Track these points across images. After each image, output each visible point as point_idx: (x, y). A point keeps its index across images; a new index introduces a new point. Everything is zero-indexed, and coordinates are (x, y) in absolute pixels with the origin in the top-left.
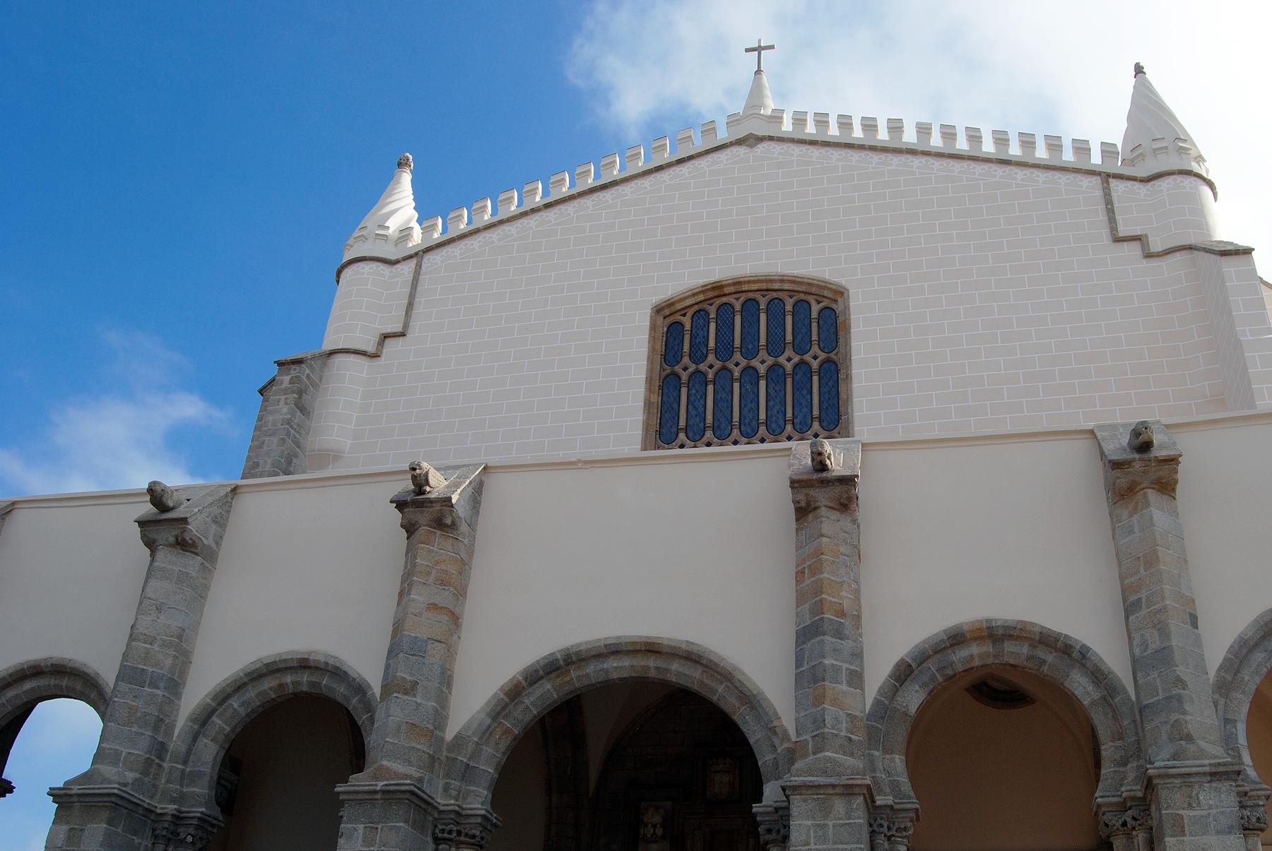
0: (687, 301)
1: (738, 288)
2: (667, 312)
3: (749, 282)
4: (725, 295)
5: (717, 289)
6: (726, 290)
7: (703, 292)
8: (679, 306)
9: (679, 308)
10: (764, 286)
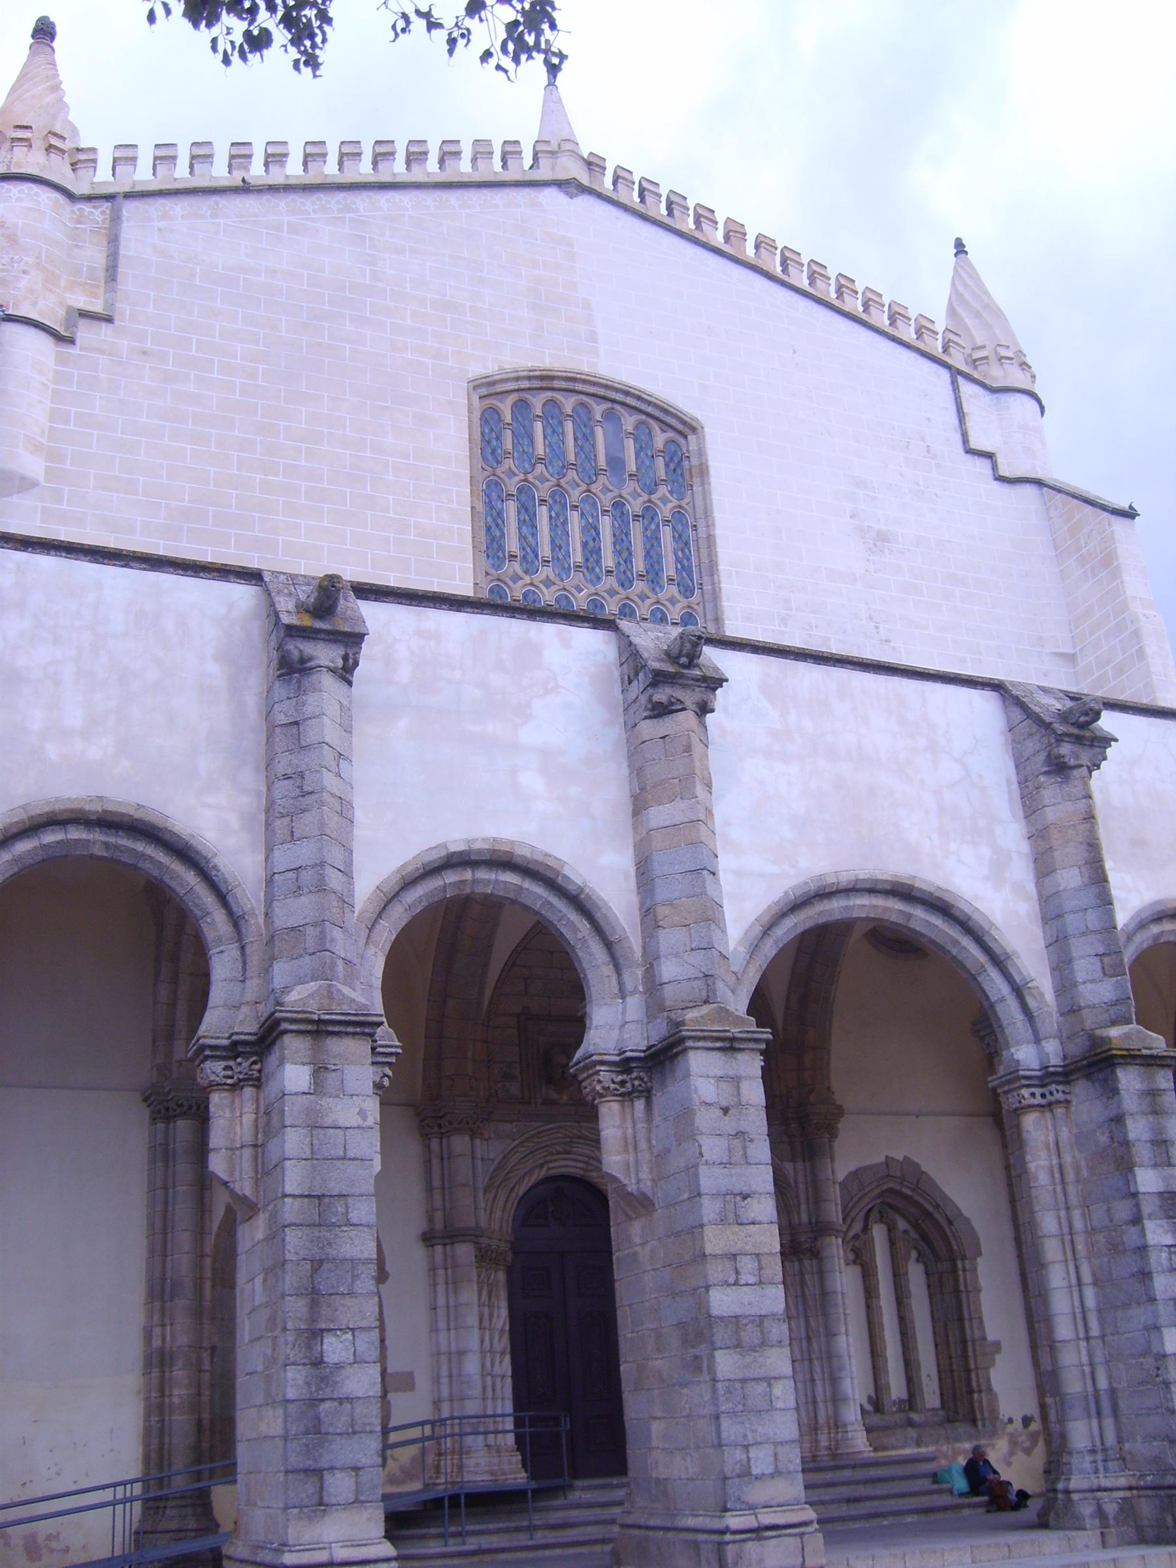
0: (509, 384)
1: (570, 385)
2: (484, 391)
3: (585, 382)
4: (552, 389)
5: (545, 381)
6: (557, 384)
7: (529, 378)
8: (500, 388)
9: (498, 390)
10: (601, 392)
